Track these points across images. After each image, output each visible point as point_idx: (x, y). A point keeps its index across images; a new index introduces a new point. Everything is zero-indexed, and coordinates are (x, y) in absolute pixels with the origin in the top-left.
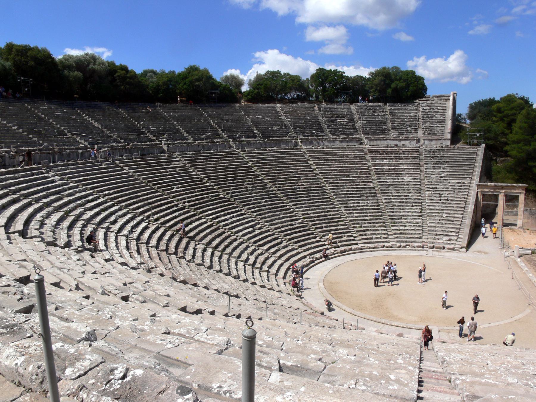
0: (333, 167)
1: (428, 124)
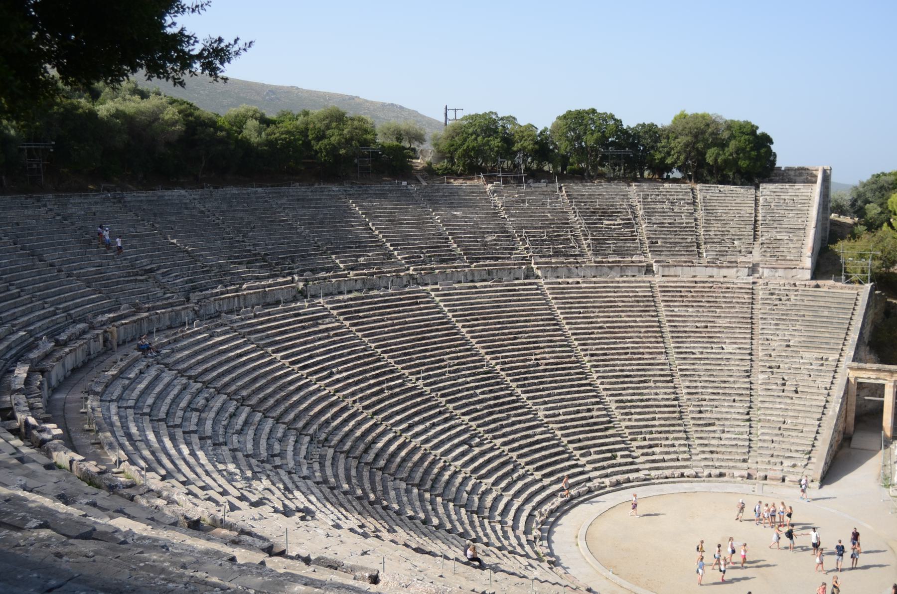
1: (773, 234)
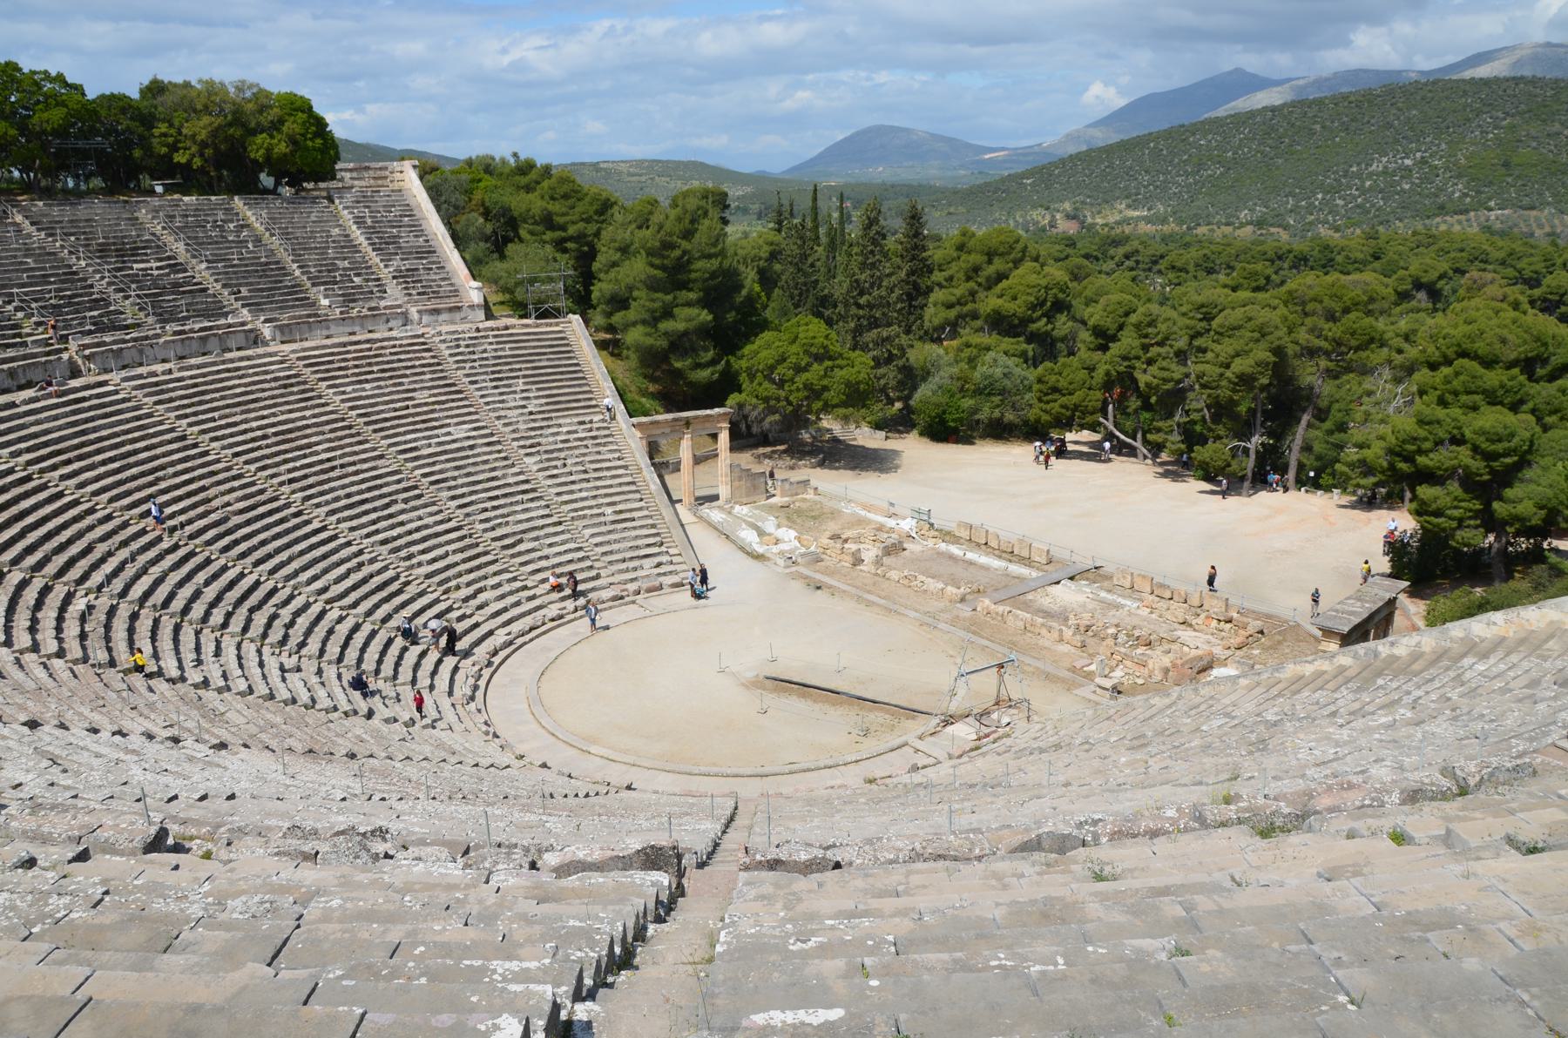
0: (252, 430)
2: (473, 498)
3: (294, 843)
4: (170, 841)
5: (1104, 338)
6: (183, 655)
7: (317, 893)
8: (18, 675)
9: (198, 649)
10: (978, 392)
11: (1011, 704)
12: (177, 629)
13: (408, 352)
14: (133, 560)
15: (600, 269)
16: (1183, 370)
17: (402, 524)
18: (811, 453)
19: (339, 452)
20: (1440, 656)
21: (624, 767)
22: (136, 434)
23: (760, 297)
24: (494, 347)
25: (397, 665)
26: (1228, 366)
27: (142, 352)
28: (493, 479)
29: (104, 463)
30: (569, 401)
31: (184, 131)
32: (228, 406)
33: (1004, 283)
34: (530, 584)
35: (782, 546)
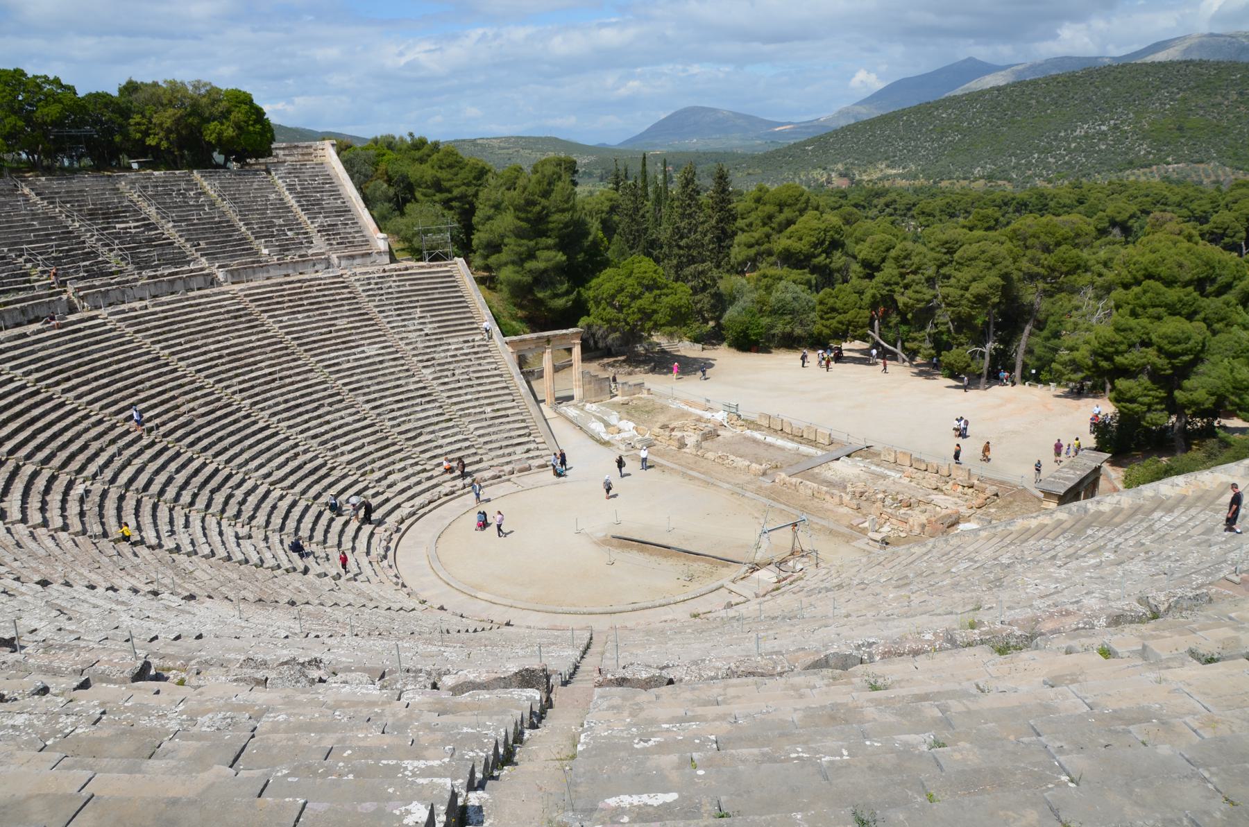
0: (210, 352)
2: (383, 401)
3: (248, 672)
4: (152, 672)
5: (870, 269)
6: (160, 528)
7: (267, 710)
8: (32, 545)
9: (171, 522)
10: (774, 312)
11: (803, 554)
12: (155, 507)
13: (331, 289)
14: (120, 454)
15: (478, 223)
16: (932, 292)
17: (328, 422)
18: (645, 362)
19: (278, 368)
20: (1136, 510)
21: (504, 609)
22: (120, 357)
23: (603, 242)
24: (398, 284)
25: (326, 532)
26: (967, 289)
27: (124, 292)
28: (398, 386)
29: (96, 379)
30: (456, 325)
31: (154, 121)
32: (191, 334)
33: (793, 228)
34: (428, 467)
35: (623, 435)
